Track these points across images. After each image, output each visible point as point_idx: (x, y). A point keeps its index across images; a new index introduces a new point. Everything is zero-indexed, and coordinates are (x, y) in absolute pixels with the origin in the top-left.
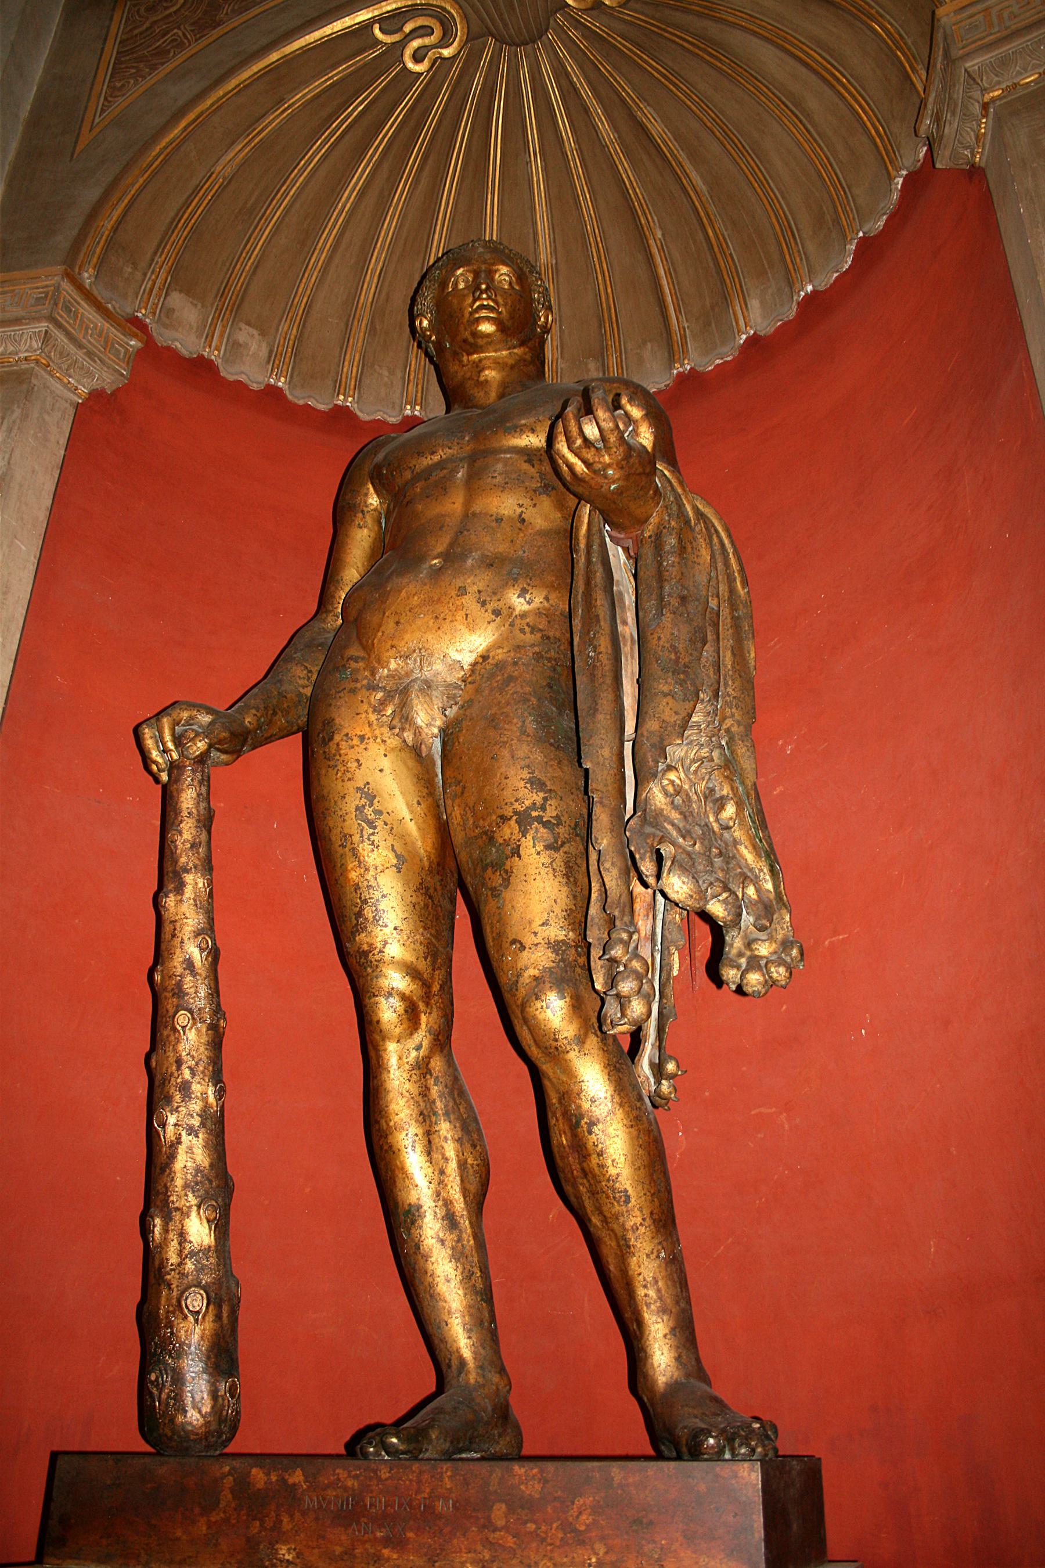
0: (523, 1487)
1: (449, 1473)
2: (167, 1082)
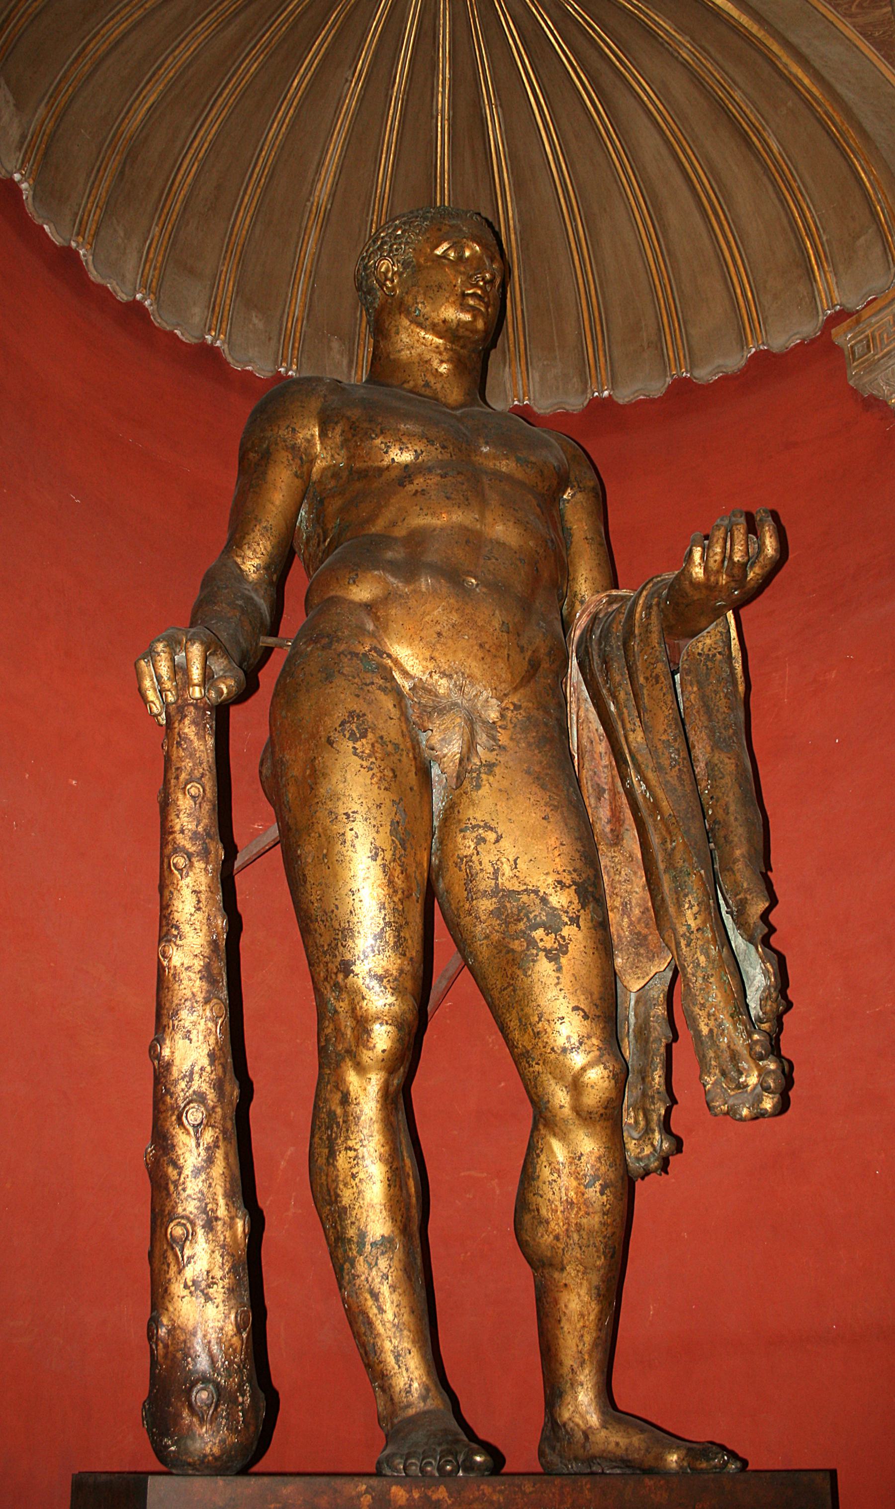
0: (652, 1496)
1: (588, 1486)
2: (196, 1077)
